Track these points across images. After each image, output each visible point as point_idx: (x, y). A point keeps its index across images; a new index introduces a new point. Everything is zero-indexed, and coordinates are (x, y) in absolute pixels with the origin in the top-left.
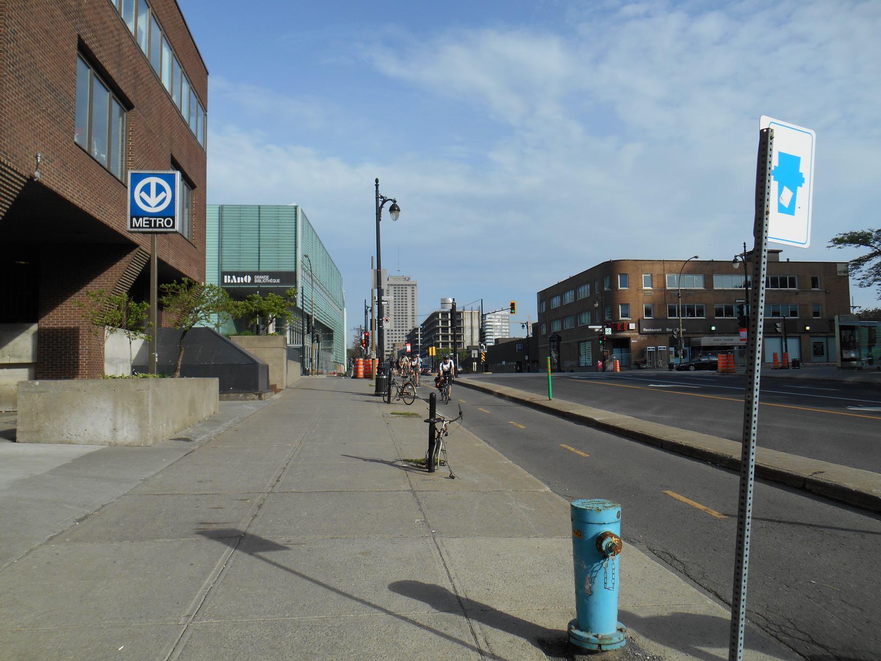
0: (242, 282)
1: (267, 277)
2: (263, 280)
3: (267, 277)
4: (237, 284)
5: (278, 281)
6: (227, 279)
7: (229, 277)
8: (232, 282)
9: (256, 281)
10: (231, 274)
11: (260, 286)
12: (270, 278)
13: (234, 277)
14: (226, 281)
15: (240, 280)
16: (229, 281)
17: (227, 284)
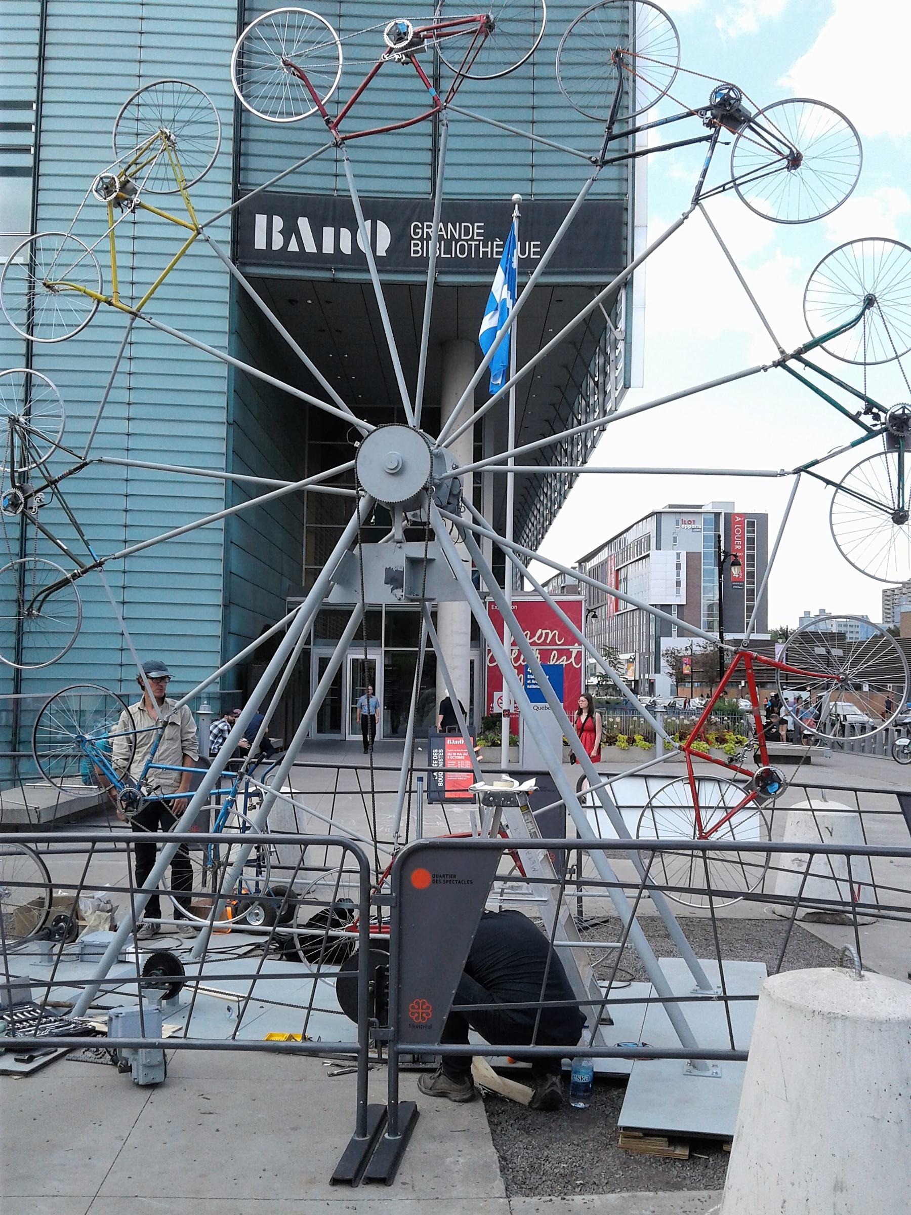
0: (346, 248)
1: (476, 229)
2: (455, 248)
3: (476, 229)
4: (319, 260)
7: (278, 223)
8: (293, 247)
13: (303, 224)
14: (260, 243)
16: (278, 242)
17: (269, 256)
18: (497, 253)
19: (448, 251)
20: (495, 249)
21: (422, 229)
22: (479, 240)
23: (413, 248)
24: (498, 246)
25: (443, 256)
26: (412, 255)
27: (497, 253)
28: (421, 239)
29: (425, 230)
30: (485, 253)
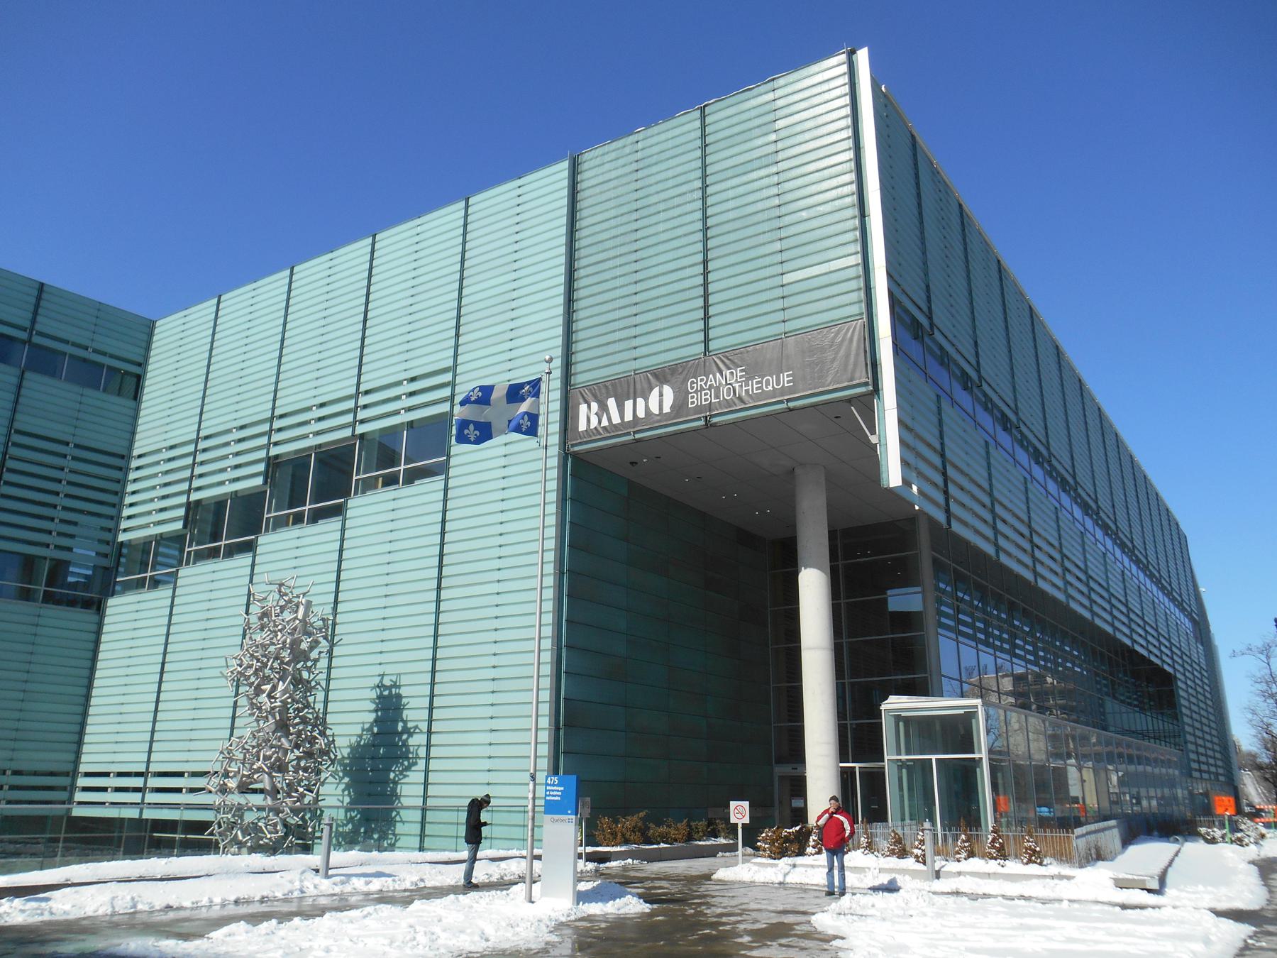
0: (641, 413)
5: (786, 379)
6: (587, 417)
8: (605, 423)
9: (693, 401)
10: (600, 392)
11: (714, 420)
12: (749, 378)
13: (611, 403)
14: (582, 426)
15: (634, 409)
18: (757, 389)
19: (717, 397)
20: (755, 386)
21: (697, 383)
22: (741, 382)
23: (690, 400)
24: (757, 383)
25: (713, 401)
26: (690, 406)
27: (757, 389)
28: (696, 392)
29: (699, 383)
30: (747, 391)
